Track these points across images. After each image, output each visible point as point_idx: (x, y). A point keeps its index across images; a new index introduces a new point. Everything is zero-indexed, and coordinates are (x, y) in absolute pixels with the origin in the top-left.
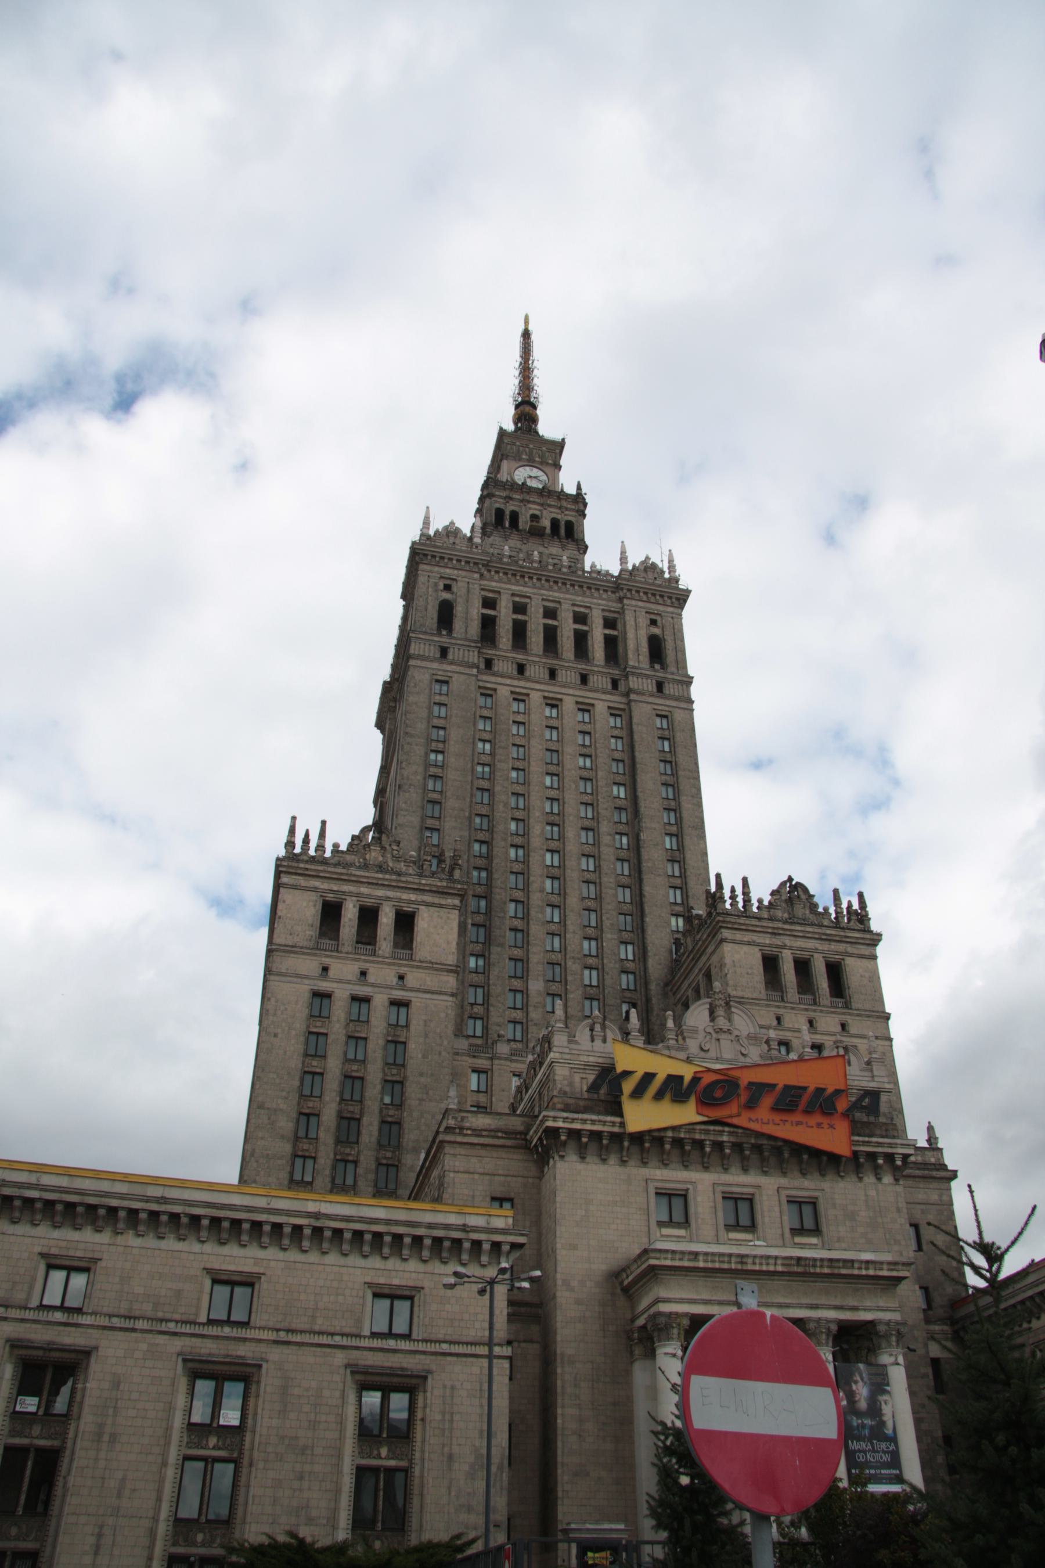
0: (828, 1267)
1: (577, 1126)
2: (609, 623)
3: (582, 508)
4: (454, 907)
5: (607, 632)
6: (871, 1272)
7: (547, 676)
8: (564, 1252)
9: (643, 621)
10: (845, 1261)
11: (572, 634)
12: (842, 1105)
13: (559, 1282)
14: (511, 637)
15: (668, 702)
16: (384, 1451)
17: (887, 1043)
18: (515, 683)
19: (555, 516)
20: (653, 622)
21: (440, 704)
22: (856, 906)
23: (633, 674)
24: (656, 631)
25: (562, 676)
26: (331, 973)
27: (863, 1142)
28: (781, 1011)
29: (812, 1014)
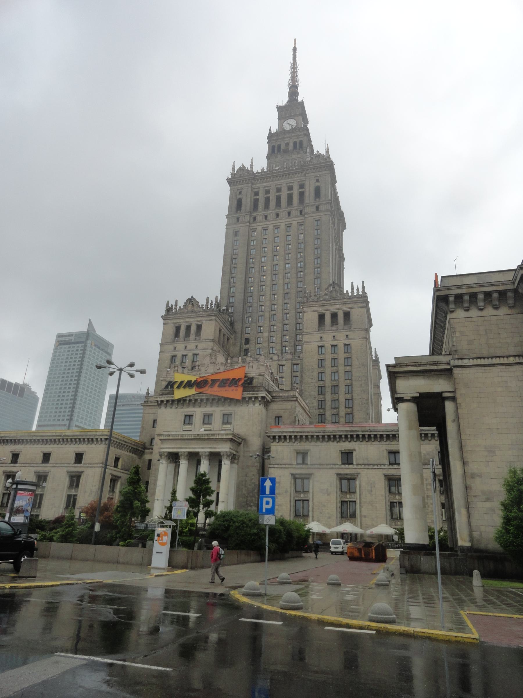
1: (163, 399)
2: (302, 186)
3: (305, 132)
4: (214, 320)
6: (220, 437)
10: (212, 434)
12: (240, 383)
14: (263, 205)
16: (73, 491)
18: (264, 223)
19: (295, 140)
20: (318, 180)
21: (237, 240)
23: (306, 206)
24: (318, 184)
28: (322, 335)
29: (334, 334)
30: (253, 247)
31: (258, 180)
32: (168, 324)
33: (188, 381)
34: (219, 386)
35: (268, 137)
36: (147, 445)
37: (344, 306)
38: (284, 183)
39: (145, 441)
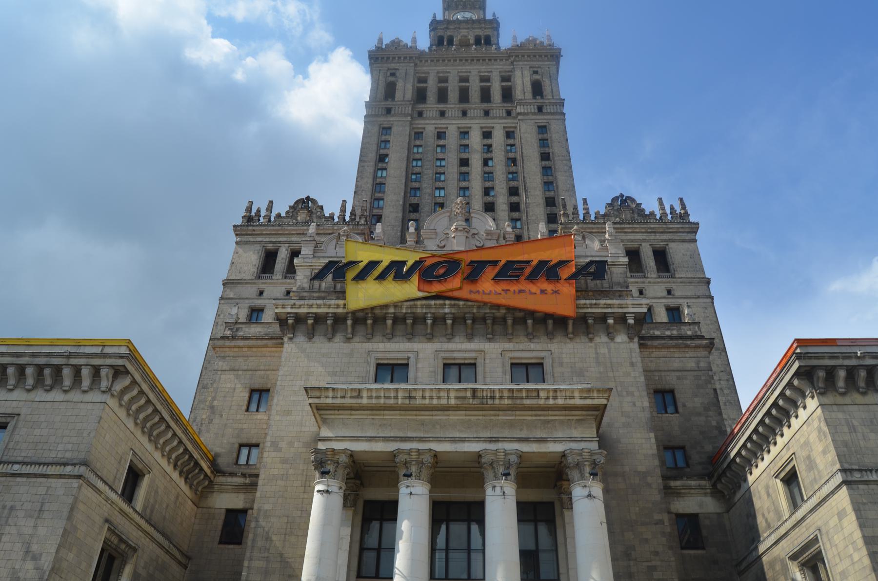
0: (509, 398)
2: (506, 79)
5: (504, 84)
6: (560, 402)
7: (460, 115)
8: (278, 418)
9: (527, 73)
11: (478, 89)
13: (268, 444)
15: (546, 117)
17: (709, 300)
18: (438, 122)
20: (536, 73)
22: (678, 209)
24: (537, 77)
25: (471, 113)
26: (265, 294)
27: (591, 304)
29: (641, 285)
30: (418, 156)
31: (426, 61)
32: (246, 243)
33: (393, 264)
34: (497, 278)
35: (431, 25)
36: (222, 462)
37: (652, 237)
38: (474, 71)
39: (218, 450)
